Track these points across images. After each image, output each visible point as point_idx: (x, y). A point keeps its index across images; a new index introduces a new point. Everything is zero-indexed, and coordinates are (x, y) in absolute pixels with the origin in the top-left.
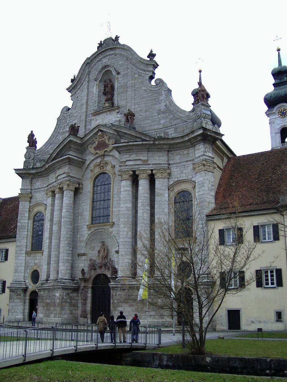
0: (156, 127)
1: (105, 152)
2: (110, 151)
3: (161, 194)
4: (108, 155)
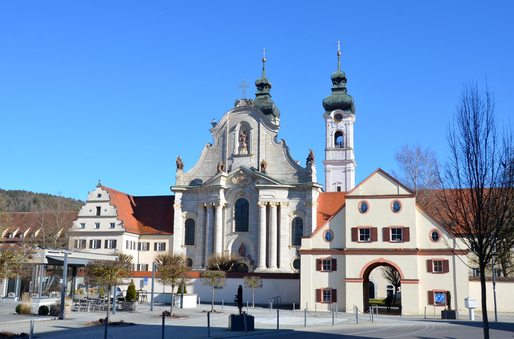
0: (280, 172)
1: (244, 185)
2: (248, 184)
3: (284, 218)
4: (246, 187)
